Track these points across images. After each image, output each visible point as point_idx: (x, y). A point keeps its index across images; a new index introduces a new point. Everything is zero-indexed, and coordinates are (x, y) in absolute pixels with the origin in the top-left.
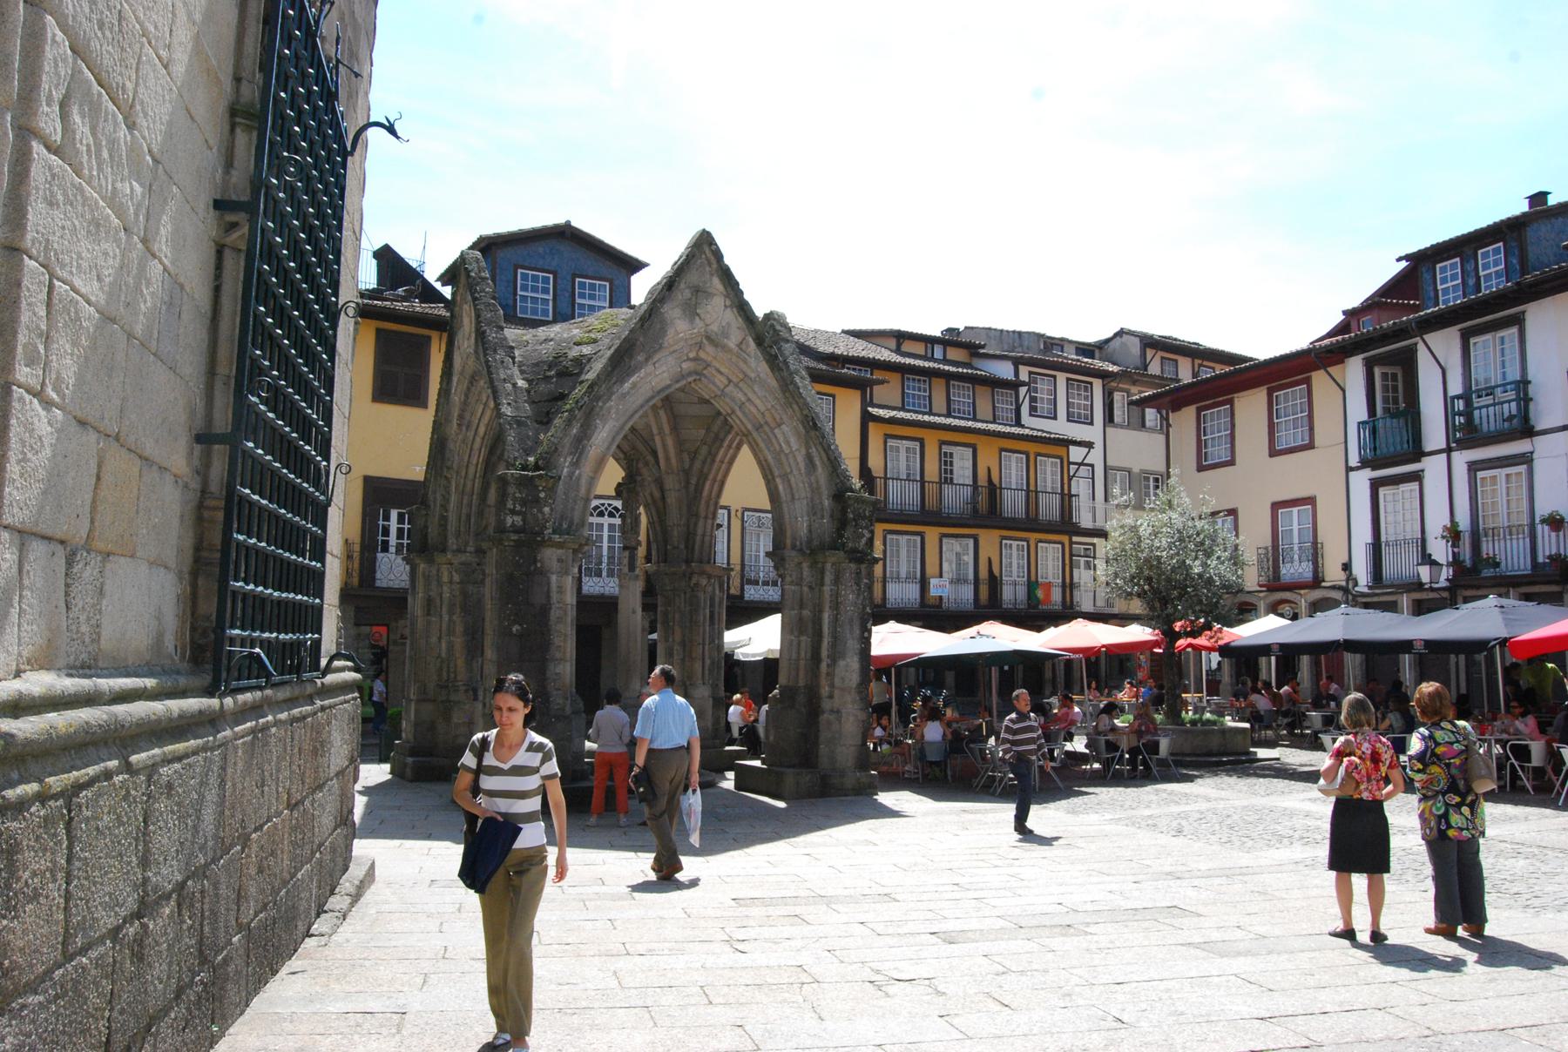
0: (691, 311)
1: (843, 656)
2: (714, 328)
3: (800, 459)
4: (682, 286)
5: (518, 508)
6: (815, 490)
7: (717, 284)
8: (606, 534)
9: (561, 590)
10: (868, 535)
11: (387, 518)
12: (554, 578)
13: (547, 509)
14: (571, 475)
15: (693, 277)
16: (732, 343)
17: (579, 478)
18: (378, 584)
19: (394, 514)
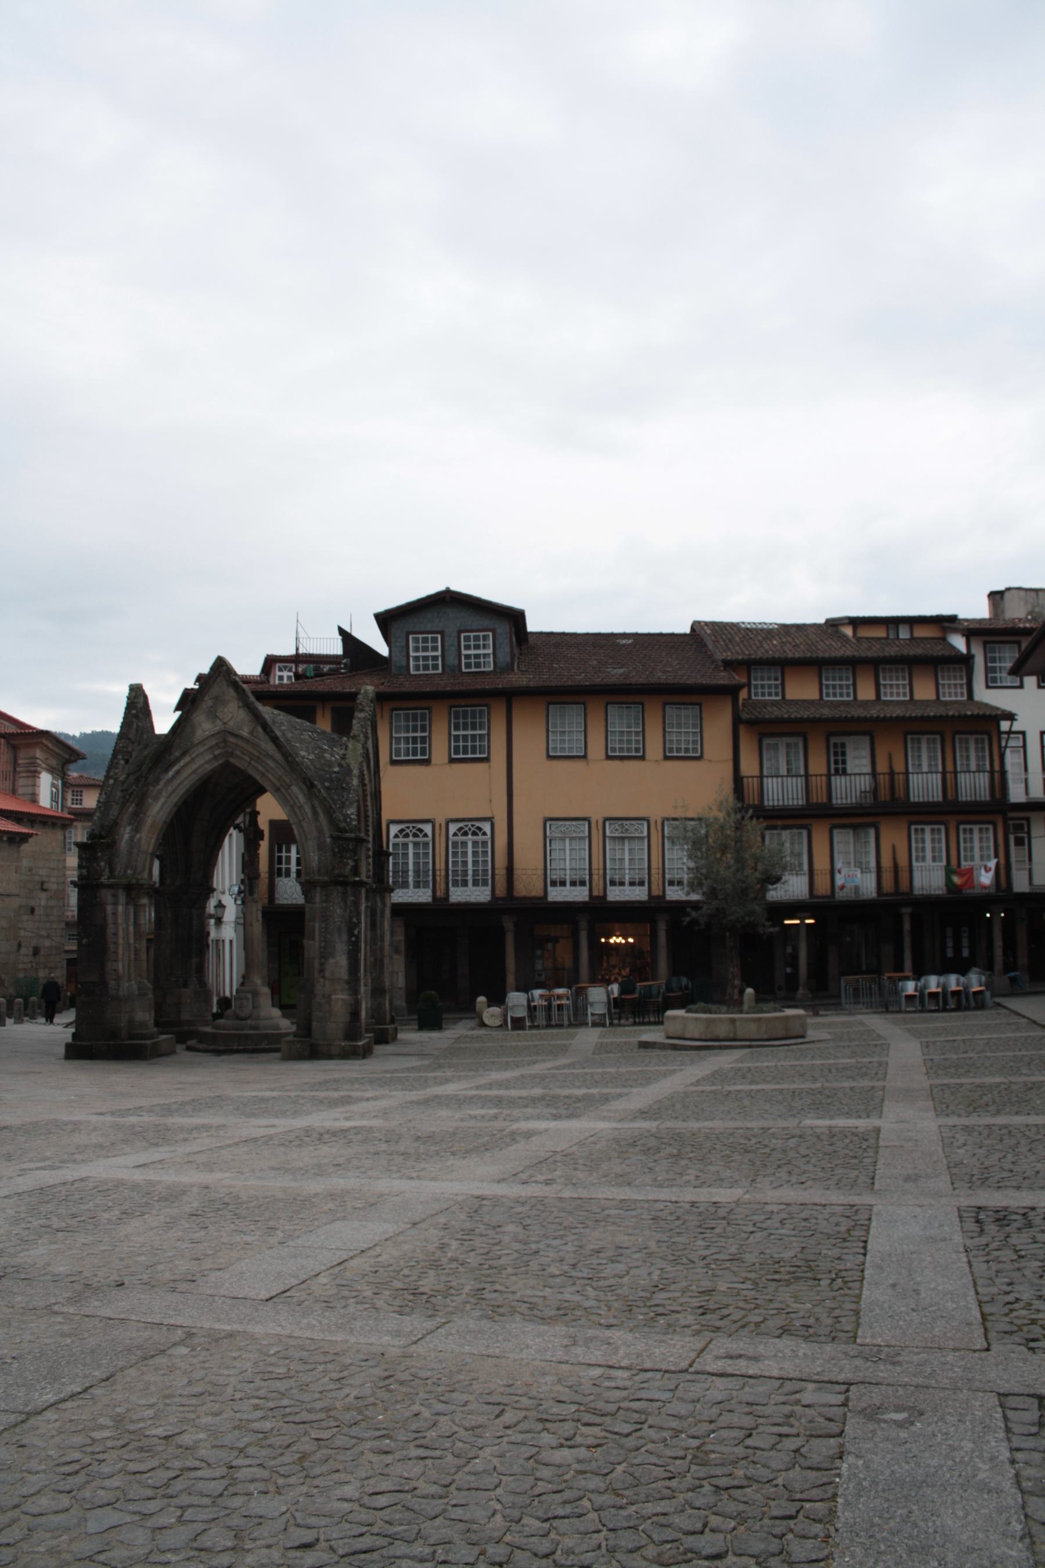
0: (213, 715)
1: (332, 955)
2: (231, 723)
3: (308, 809)
4: (206, 698)
5: (84, 864)
6: (320, 832)
7: (231, 693)
8: (470, 850)
9: (115, 914)
10: (351, 863)
11: (288, 851)
12: (109, 909)
13: (102, 864)
14: (132, 838)
15: (215, 690)
16: (245, 732)
17: (140, 839)
18: (277, 902)
19: (294, 849)
